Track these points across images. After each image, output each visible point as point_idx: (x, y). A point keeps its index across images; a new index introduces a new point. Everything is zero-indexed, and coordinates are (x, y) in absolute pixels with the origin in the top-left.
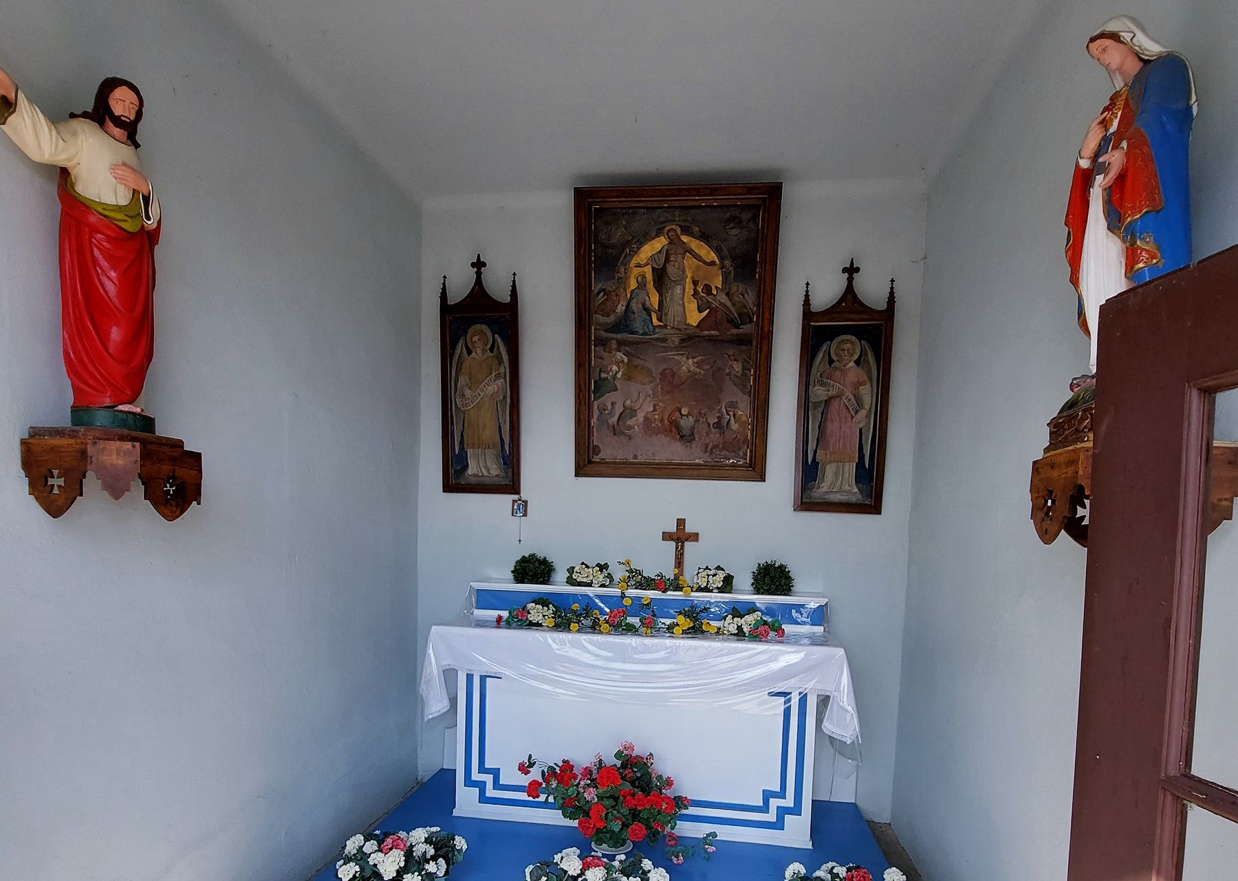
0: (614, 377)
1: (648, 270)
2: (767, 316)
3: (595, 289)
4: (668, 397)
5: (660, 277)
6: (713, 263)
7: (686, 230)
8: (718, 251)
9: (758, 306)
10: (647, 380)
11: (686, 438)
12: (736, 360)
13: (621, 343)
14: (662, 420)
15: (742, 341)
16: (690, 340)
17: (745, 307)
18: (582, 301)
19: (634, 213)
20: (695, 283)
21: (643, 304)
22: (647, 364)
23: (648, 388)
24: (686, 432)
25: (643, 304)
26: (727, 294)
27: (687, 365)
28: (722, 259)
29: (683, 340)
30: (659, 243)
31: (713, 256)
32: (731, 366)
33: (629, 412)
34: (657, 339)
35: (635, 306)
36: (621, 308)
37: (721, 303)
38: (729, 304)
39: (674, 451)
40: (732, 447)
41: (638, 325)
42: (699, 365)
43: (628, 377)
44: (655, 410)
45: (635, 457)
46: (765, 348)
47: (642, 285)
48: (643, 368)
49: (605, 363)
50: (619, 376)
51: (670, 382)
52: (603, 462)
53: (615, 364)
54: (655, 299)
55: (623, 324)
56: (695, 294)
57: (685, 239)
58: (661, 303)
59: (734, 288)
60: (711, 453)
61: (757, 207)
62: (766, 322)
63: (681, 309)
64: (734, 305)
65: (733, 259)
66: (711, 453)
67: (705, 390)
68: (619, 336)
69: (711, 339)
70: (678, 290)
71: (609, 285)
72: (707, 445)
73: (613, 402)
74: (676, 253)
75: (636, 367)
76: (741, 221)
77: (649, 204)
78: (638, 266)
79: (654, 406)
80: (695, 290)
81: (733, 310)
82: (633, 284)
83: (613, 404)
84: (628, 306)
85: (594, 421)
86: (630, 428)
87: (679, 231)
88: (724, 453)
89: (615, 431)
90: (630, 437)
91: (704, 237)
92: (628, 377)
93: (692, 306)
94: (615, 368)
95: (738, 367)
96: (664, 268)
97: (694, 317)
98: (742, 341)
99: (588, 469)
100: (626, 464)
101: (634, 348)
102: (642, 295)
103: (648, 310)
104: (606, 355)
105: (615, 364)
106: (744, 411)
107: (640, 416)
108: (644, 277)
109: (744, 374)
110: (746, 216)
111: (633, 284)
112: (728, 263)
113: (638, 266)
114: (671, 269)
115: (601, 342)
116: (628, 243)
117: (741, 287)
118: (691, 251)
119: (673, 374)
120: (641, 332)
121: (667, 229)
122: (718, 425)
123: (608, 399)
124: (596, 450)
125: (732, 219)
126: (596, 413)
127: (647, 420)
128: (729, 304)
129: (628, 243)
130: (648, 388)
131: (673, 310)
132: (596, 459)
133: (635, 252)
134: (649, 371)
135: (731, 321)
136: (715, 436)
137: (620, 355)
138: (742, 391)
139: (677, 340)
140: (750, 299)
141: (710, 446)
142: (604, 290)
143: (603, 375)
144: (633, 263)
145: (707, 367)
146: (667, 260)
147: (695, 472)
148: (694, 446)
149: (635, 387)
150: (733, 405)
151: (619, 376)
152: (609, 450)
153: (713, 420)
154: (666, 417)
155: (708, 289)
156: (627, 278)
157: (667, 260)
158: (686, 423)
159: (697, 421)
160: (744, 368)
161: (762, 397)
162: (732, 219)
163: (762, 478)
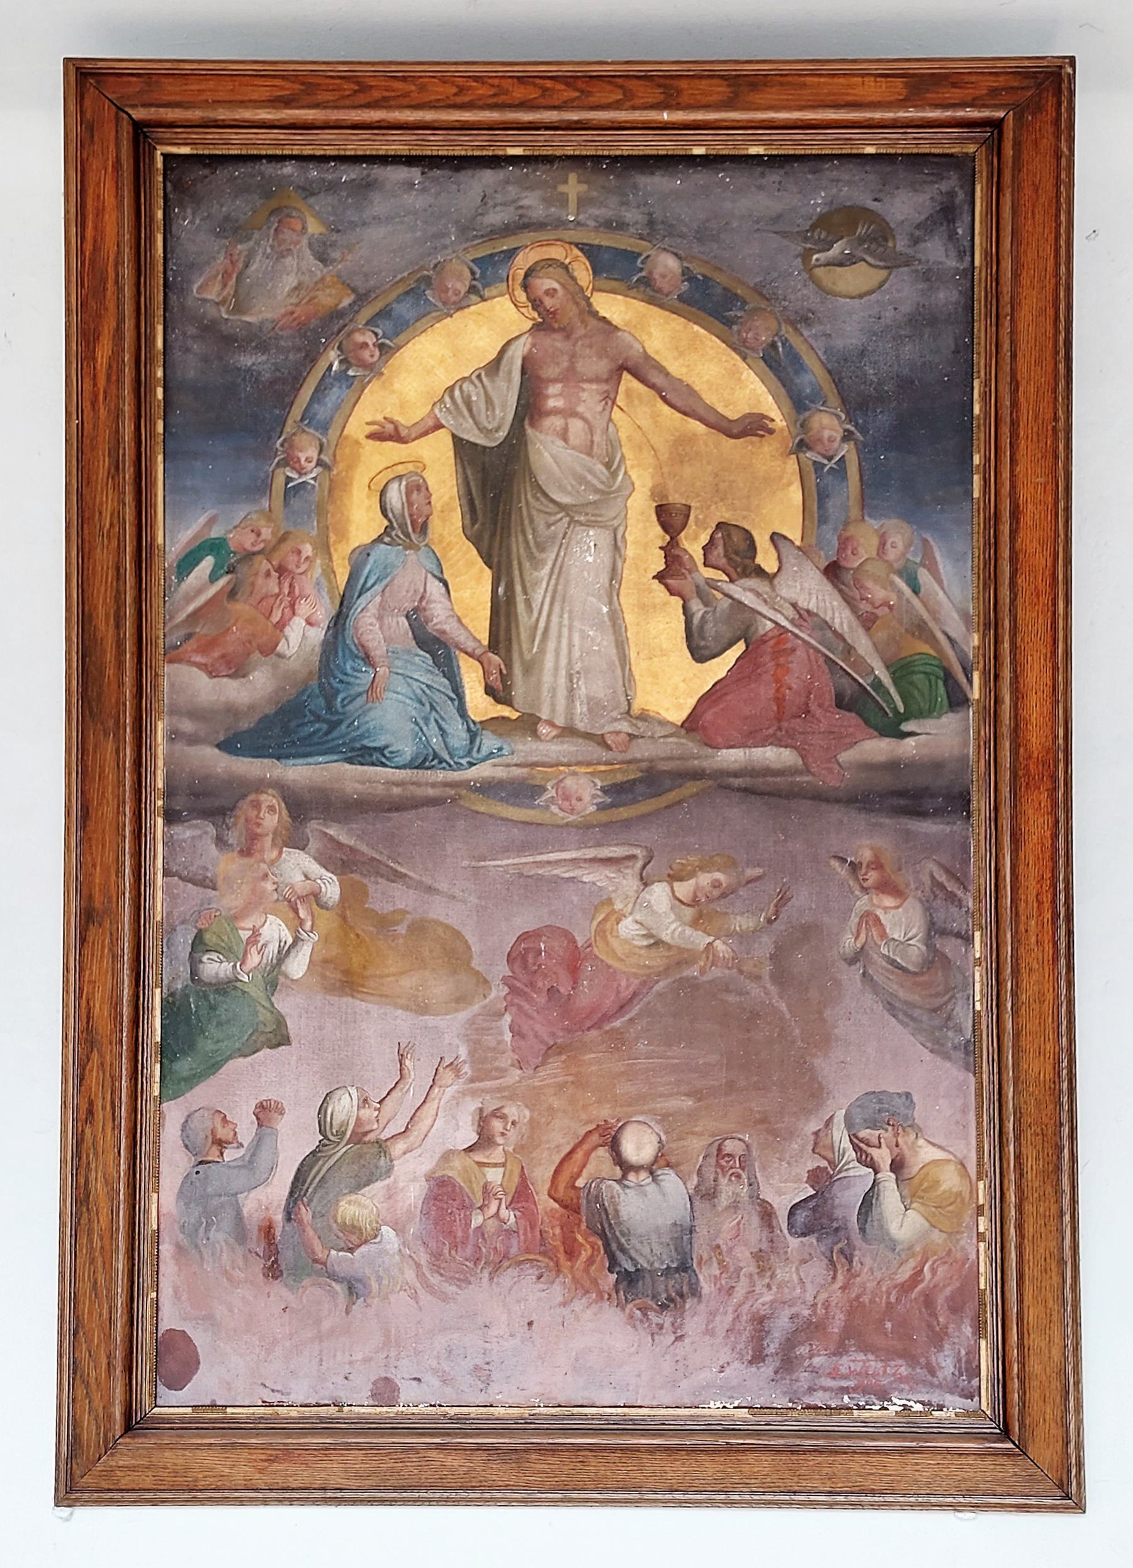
0: (273, 977)
1: (437, 464)
2: (1036, 676)
3: (173, 536)
4: (554, 1069)
5: (496, 485)
6: (753, 427)
7: (618, 268)
8: (778, 364)
9: (991, 624)
10: (440, 988)
11: (652, 1286)
12: (887, 887)
13: (302, 807)
14: (521, 1195)
15: (910, 796)
16: (650, 793)
17: (921, 630)
18: (104, 627)
19: (366, 187)
20: (670, 518)
21: (417, 619)
22: (439, 911)
23: (450, 1031)
24: (650, 1253)
25: (417, 619)
26: (833, 572)
27: (645, 914)
28: (799, 403)
29: (618, 793)
30: (491, 326)
31: (750, 391)
32: (870, 919)
33: (349, 1152)
34: (487, 788)
35: (377, 627)
36: (302, 637)
37: (803, 616)
38: (841, 617)
39: (571, 1353)
40: (896, 1327)
41: (392, 714)
42: (701, 911)
43: (345, 977)
44: (485, 1140)
45: (385, 1391)
46: (1036, 827)
47: (407, 527)
48: (419, 928)
49: (230, 901)
50: (298, 966)
51: (554, 990)
52: (214, 1424)
53: (262, 907)
54: (467, 597)
55: (309, 718)
56: (673, 570)
57: (614, 307)
58: (502, 612)
59: (866, 536)
60: (788, 1363)
61: (961, 165)
62: (1036, 708)
63: (604, 643)
64: (868, 622)
65: (857, 405)
66: (788, 1363)
67: (747, 1038)
68: (298, 772)
69: (759, 790)
70: (587, 552)
71: (240, 523)
72: (760, 1323)
73: (264, 1104)
74: (570, 377)
75: (384, 923)
76: (882, 233)
77: (437, 145)
78: (388, 433)
79: (483, 1122)
80: (672, 554)
81: (863, 645)
82: (362, 522)
83: (265, 1113)
84: (339, 621)
85: (165, 1202)
86: (356, 1237)
87: (583, 273)
88: (853, 1361)
89: (275, 1254)
90: (354, 1288)
91: (710, 302)
92: (345, 977)
93: (660, 626)
94: (275, 931)
95: (902, 923)
96: (514, 448)
97: (672, 685)
98: (910, 796)
99: (129, 1454)
100: (331, 1428)
101: (373, 832)
102: (409, 574)
103: (436, 647)
104: (226, 865)
105: (262, 907)
106: (947, 1139)
107: (410, 1175)
108: (417, 488)
109: (935, 960)
110: (905, 206)
111: (362, 522)
112: (828, 424)
113: (388, 433)
114: (551, 453)
115: (208, 803)
116: (333, 324)
117: (900, 537)
118: (640, 368)
119: (575, 961)
120: (408, 750)
121: (523, 261)
122: (816, 1217)
123: (237, 1088)
124: (177, 1359)
125: (838, 222)
126: (173, 1164)
127: (444, 1195)
128: (841, 617)
129: (333, 324)
130: (450, 1031)
131: (566, 661)
132: (173, 1403)
133: (362, 370)
134: (455, 954)
135: (857, 703)
136: (802, 1279)
137: (299, 867)
138: (938, 1048)
139: (586, 792)
140: (949, 594)
141: (781, 1325)
142: (215, 547)
143: (214, 967)
144: (357, 425)
145: (742, 922)
146: (530, 408)
147: (710, 1469)
148: (693, 1324)
149: (377, 1027)
150: (887, 1113)
151: (298, 966)
152: (244, 1353)
153: (785, 1190)
154: (542, 1176)
155: (736, 550)
156: (336, 488)
157: (530, 408)
158: (649, 1209)
159: (705, 1194)
160: (934, 930)
161: (1037, 1068)
162: (838, 222)
163: (1080, 1507)
